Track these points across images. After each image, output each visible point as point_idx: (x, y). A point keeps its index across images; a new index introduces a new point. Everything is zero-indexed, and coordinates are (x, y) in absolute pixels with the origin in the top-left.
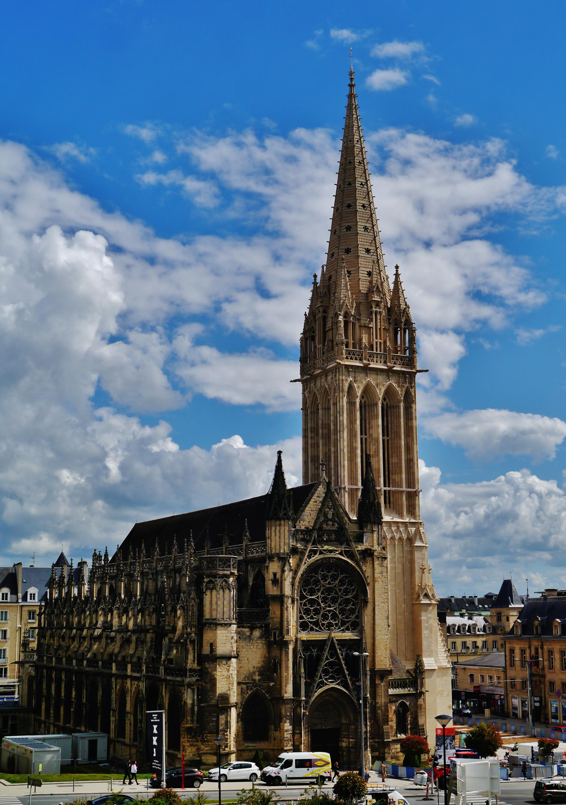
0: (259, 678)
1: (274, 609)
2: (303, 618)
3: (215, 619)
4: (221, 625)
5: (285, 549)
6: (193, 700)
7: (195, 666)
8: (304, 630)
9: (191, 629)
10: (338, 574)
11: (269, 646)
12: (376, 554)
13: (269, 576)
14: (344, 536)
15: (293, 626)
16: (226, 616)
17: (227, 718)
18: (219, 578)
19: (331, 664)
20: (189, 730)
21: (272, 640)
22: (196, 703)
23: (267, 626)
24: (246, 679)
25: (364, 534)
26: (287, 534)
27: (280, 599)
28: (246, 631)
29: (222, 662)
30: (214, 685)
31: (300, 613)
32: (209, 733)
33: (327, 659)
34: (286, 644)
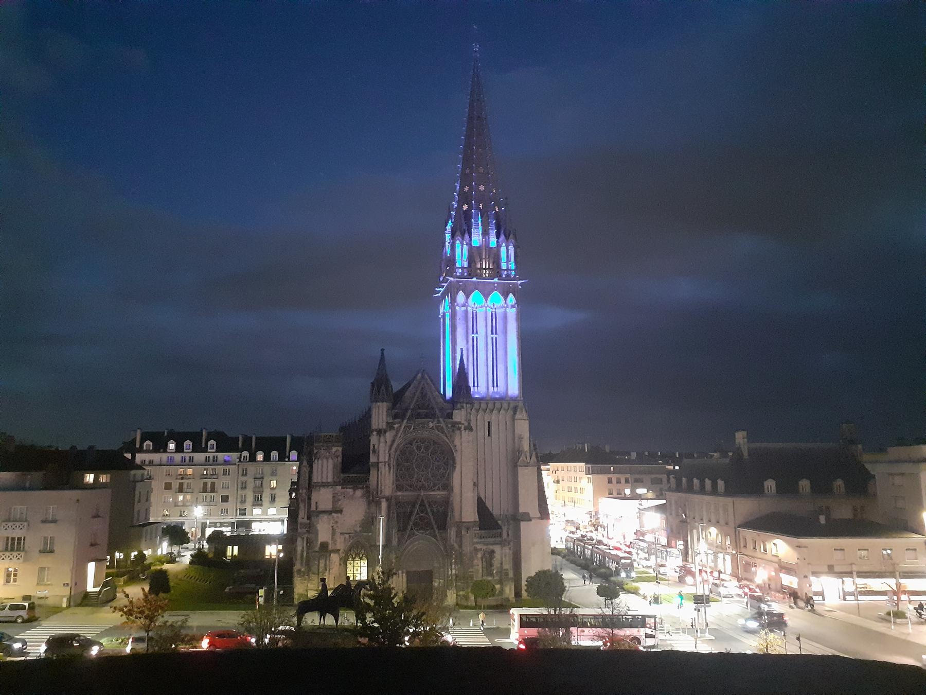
0: (361, 529)
1: (373, 472)
2: (399, 481)
3: (319, 483)
4: (324, 486)
5: (383, 426)
6: (303, 548)
7: (306, 521)
8: (400, 490)
9: (302, 490)
10: (431, 445)
11: (369, 503)
12: (463, 427)
13: (372, 447)
14: (435, 414)
15: (389, 487)
16: (330, 480)
17: (326, 562)
18: (324, 449)
19: (422, 519)
20: (299, 571)
21: (371, 498)
22: (305, 549)
23: (368, 487)
24: (349, 530)
25: (454, 412)
26: (385, 413)
27: (377, 464)
28: (350, 491)
29: (323, 517)
30: (317, 534)
31: (397, 476)
32: (313, 574)
33: (418, 514)
34: (378, 504)
